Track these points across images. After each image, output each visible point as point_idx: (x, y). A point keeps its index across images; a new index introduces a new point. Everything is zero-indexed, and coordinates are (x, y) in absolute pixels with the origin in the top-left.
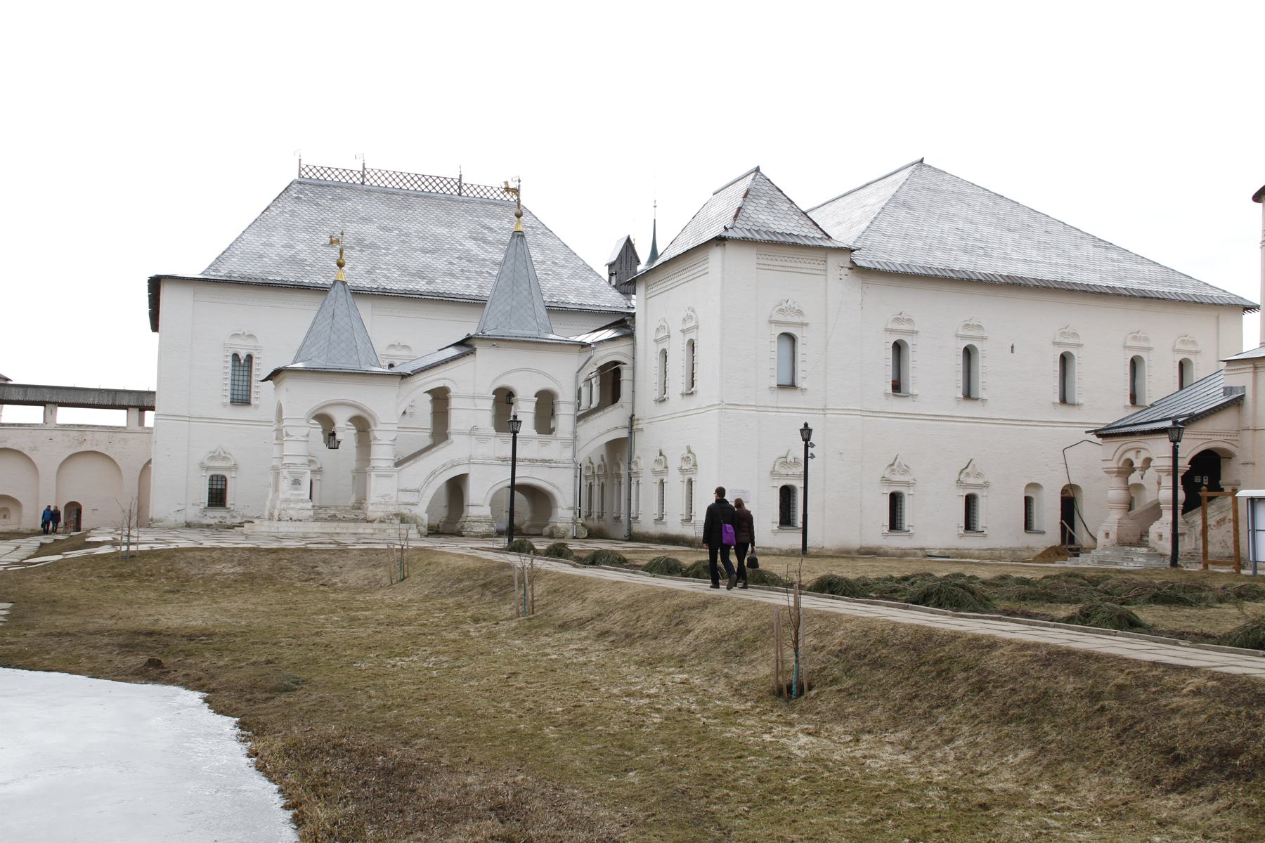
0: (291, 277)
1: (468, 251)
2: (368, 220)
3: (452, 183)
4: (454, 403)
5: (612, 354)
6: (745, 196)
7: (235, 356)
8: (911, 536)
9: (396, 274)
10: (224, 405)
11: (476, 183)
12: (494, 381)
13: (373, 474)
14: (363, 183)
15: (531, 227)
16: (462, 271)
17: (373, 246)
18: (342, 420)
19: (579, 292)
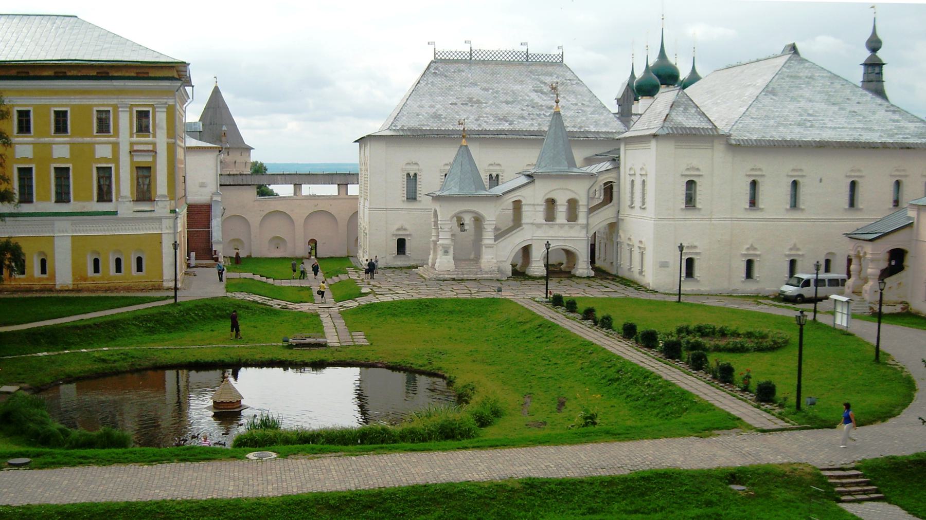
0: (434, 125)
1: (532, 100)
2: (475, 84)
3: (523, 54)
4: (524, 208)
5: (607, 178)
6: (671, 107)
7: (408, 175)
8: (758, 282)
9: (491, 120)
10: (403, 201)
11: (537, 53)
12: (545, 195)
13: (484, 246)
14: (471, 59)
15: (570, 80)
16: (529, 114)
17: (478, 102)
18: (468, 220)
19: (596, 123)
